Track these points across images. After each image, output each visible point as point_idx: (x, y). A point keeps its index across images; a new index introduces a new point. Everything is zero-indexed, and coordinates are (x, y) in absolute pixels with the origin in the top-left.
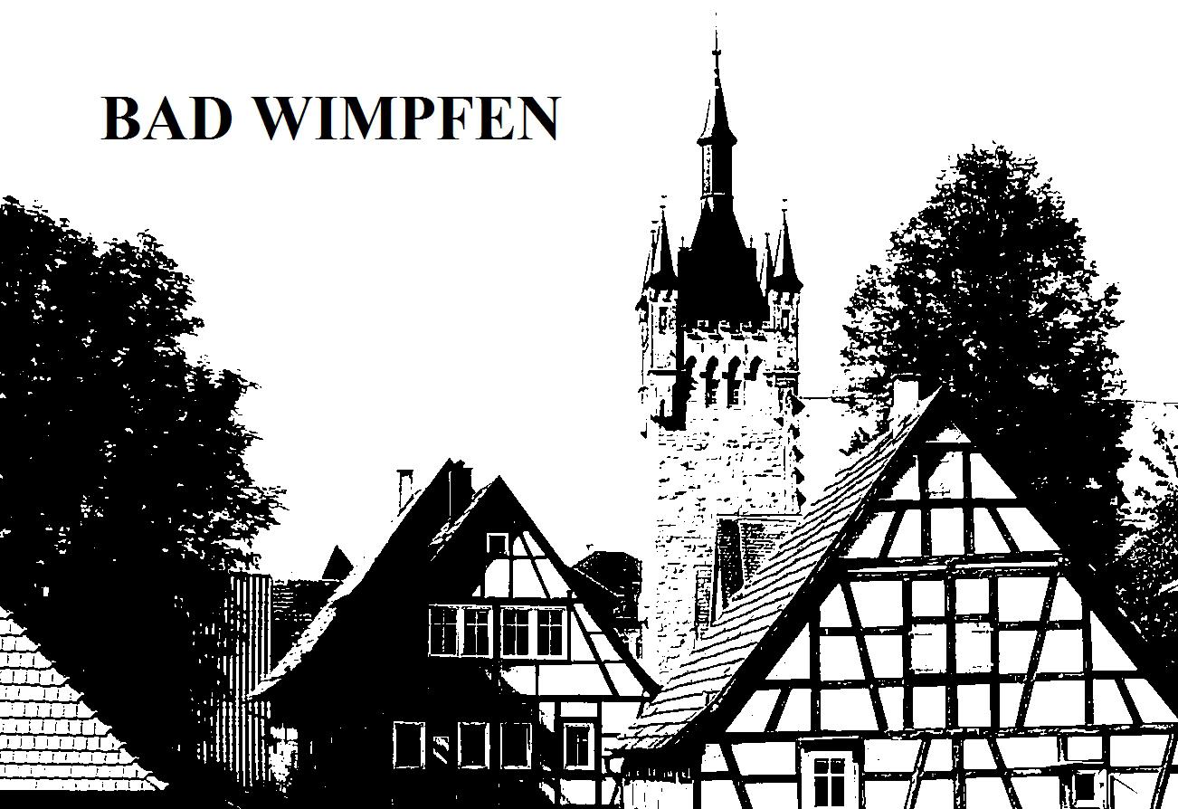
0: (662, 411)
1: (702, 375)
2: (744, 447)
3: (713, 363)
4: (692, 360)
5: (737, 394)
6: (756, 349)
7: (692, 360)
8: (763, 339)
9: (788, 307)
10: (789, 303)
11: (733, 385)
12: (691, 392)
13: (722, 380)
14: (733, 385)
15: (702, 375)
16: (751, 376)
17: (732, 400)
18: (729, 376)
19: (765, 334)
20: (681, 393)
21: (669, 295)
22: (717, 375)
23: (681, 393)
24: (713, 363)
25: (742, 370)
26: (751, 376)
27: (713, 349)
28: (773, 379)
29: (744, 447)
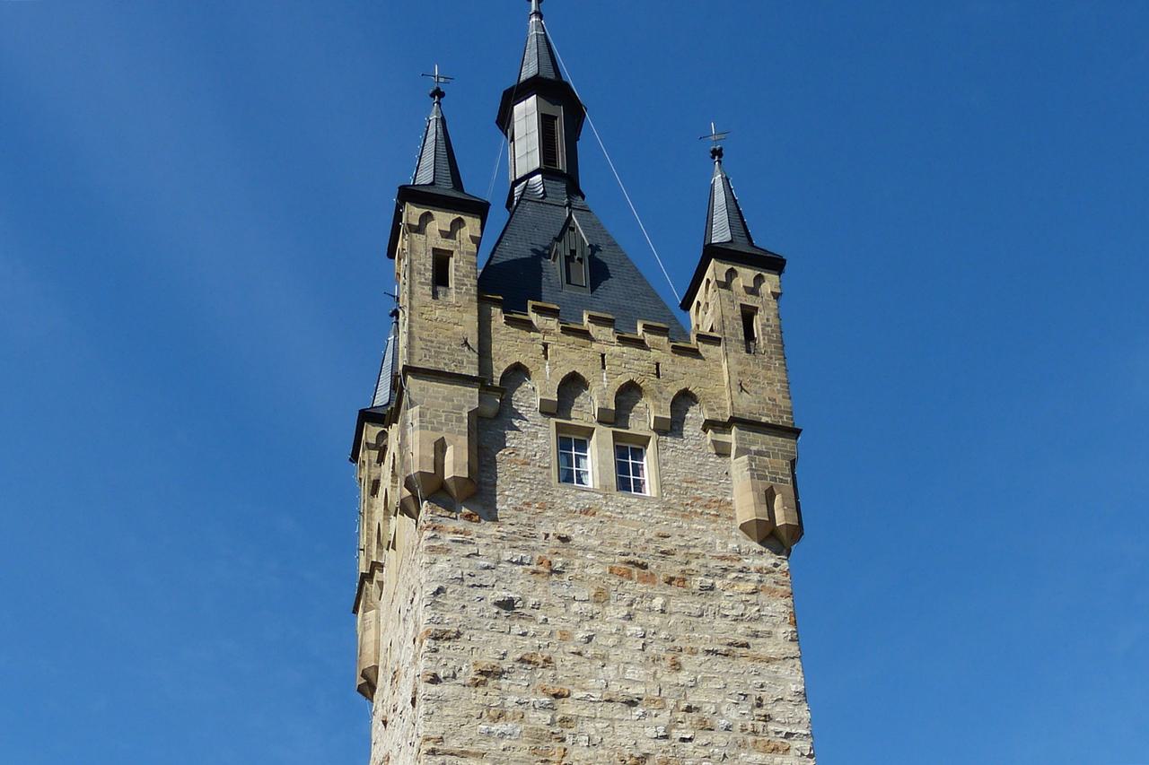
0: (439, 464)
1: (547, 410)
2: (670, 581)
3: (573, 385)
4: (518, 373)
5: (637, 470)
6: (682, 373)
7: (518, 373)
8: (695, 353)
9: (750, 301)
10: (753, 291)
11: (628, 453)
12: (510, 434)
13: (599, 428)
14: (628, 453)
15: (547, 410)
16: (671, 427)
17: (627, 479)
18: (616, 416)
19: (702, 347)
20: (489, 429)
21: (458, 224)
22: (586, 410)
23: (489, 429)
24: (573, 385)
25: (643, 420)
26: (671, 427)
27: (568, 357)
28: (732, 438)
29: (670, 581)
